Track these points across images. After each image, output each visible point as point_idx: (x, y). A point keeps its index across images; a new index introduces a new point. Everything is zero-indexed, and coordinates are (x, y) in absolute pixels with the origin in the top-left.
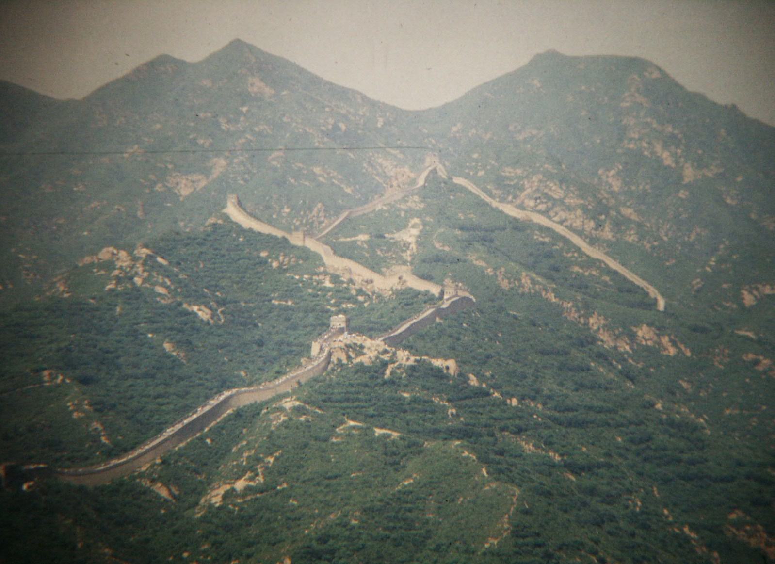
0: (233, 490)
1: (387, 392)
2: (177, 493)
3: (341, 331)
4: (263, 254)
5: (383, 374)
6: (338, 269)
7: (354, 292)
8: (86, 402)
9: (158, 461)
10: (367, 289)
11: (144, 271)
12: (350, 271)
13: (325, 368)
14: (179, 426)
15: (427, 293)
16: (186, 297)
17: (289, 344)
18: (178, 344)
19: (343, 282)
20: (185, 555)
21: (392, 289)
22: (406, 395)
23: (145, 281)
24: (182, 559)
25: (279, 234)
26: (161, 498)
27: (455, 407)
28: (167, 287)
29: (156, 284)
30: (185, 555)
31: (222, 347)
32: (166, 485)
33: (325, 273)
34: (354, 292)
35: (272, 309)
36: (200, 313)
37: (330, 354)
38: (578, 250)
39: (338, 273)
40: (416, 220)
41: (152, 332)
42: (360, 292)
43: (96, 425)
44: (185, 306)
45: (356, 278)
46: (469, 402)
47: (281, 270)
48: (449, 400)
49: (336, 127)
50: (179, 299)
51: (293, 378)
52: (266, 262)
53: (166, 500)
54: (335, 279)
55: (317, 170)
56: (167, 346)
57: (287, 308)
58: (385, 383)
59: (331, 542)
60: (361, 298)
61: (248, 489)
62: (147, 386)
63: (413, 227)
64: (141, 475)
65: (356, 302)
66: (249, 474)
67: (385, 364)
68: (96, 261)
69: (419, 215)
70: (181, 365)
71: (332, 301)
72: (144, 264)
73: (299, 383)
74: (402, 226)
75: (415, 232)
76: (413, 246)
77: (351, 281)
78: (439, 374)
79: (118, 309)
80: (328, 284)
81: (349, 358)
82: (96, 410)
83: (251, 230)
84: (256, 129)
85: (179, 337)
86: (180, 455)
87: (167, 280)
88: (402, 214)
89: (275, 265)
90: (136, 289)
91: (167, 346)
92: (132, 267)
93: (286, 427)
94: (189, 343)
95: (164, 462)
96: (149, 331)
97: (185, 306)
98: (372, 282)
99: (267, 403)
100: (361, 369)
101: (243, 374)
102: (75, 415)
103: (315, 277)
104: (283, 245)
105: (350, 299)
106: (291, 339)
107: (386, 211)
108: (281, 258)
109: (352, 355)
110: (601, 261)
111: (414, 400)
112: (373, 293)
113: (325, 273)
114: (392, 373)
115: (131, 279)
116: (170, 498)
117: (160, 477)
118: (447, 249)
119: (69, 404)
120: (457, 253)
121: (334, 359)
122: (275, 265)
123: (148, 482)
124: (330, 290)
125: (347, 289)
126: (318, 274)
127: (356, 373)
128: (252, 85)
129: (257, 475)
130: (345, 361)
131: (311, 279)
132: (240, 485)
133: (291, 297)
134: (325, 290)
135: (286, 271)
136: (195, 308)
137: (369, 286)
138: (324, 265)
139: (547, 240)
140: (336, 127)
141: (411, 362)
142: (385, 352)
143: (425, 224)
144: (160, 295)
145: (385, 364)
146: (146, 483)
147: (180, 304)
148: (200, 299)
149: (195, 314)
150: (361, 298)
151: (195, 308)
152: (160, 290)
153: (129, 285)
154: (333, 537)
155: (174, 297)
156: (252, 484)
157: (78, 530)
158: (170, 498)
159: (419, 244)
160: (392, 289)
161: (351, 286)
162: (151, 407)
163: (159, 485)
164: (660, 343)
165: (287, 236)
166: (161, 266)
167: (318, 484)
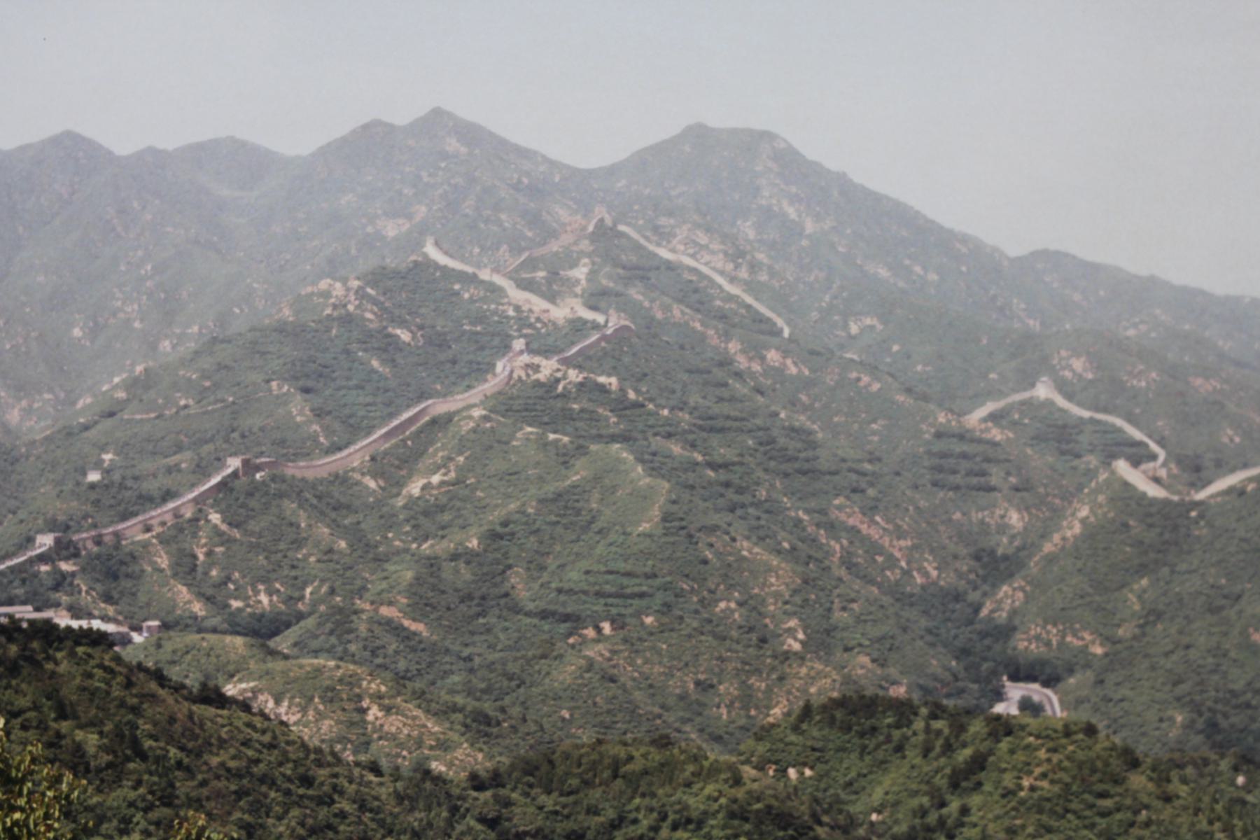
0: (430, 483)
1: (559, 404)
3: (522, 352)
4: (457, 287)
5: (556, 388)
7: (533, 320)
9: (367, 458)
10: (544, 317)
12: (528, 301)
13: (508, 383)
14: (383, 431)
15: (594, 321)
16: (393, 321)
17: (479, 363)
18: (383, 362)
20: (390, 535)
22: (575, 406)
23: (357, 307)
25: (469, 269)
28: (375, 314)
30: (390, 535)
32: (374, 477)
33: (510, 304)
34: (533, 320)
35: (464, 332)
36: (403, 336)
37: (512, 372)
38: (720, 287)
40: (586, 260)
42: (538, 320)
43: (316, 427)
44: (390, 329)
45: (535, 309)
46: (628, 412)
47: (472, 300)
48: (611, 411)
49: (519, 181)
50: (385, 324)
54: (518, 308)
55: (503, 217)
56: (375, 363)
57: (477, 333)
58: (558, 396)
59: (512, 526)
60: (539, 325)
61: (442, 483)
62: (358, 395)
63: (585, 265)
64: (353, 470)
66: (443, 471)
67: (558, 381)
69: (589, 255)
70: (387, 379)
73: (486, 396)
74: (573, 265)
75: (585, 270)
76: (583, 282)
77: (531, 311)
78: (603, 389)
79: (334, 331)
80: (511, 313)
81: (528, 375)
83: (445, 267)
85: (384, 356)
86: (386, 453)
88: (575, 255)
90: (349, 314)
91: (375, 363)
94: (393, 361)
95: (373, 459)
96: (359, 349)
97: (390, 329)
98: (548, 311)
99: (458, 412)
100: (538, 384)
101: (439, 387)
102: (298, 419)
104: (472, 279)
105: (531, 326)
106: (479, 359)
109: (530, 372)
110: (738, 297)
111: (582, 410)
113: (510, 304)
114: (564, 388)
115: (345, 306)
118: (611, 285)
120: (620, 288)
121: (515, 376)
122: (466, 296)
125: (528, 317)
126: (503, 304)
127: (534, 387)
130: (524, 378)
132: (436, 479)
133: (481, 323)
134: (507, 317)
135: (476, 301)
136: (398, 332)
138: (507, 297)
139: (694, 278)
140: (519, 181)
141: (580, 379)
142: (558, 370)
143: (593, 263)
145: (558, 381)
146: (357, 476)
147: (385, 328)
148: (403, 323)
150: (539, 325)
151: (398, 332)
152: (369, 315)
153: (343, 311)
154: (514, 522)
155: (381, 321)
156: (446, 478)
157: (301, 512)
159: (588, 280)
162: (361, 413)
164: (784, 364)
165: (477, 272)
167: (501, 479)
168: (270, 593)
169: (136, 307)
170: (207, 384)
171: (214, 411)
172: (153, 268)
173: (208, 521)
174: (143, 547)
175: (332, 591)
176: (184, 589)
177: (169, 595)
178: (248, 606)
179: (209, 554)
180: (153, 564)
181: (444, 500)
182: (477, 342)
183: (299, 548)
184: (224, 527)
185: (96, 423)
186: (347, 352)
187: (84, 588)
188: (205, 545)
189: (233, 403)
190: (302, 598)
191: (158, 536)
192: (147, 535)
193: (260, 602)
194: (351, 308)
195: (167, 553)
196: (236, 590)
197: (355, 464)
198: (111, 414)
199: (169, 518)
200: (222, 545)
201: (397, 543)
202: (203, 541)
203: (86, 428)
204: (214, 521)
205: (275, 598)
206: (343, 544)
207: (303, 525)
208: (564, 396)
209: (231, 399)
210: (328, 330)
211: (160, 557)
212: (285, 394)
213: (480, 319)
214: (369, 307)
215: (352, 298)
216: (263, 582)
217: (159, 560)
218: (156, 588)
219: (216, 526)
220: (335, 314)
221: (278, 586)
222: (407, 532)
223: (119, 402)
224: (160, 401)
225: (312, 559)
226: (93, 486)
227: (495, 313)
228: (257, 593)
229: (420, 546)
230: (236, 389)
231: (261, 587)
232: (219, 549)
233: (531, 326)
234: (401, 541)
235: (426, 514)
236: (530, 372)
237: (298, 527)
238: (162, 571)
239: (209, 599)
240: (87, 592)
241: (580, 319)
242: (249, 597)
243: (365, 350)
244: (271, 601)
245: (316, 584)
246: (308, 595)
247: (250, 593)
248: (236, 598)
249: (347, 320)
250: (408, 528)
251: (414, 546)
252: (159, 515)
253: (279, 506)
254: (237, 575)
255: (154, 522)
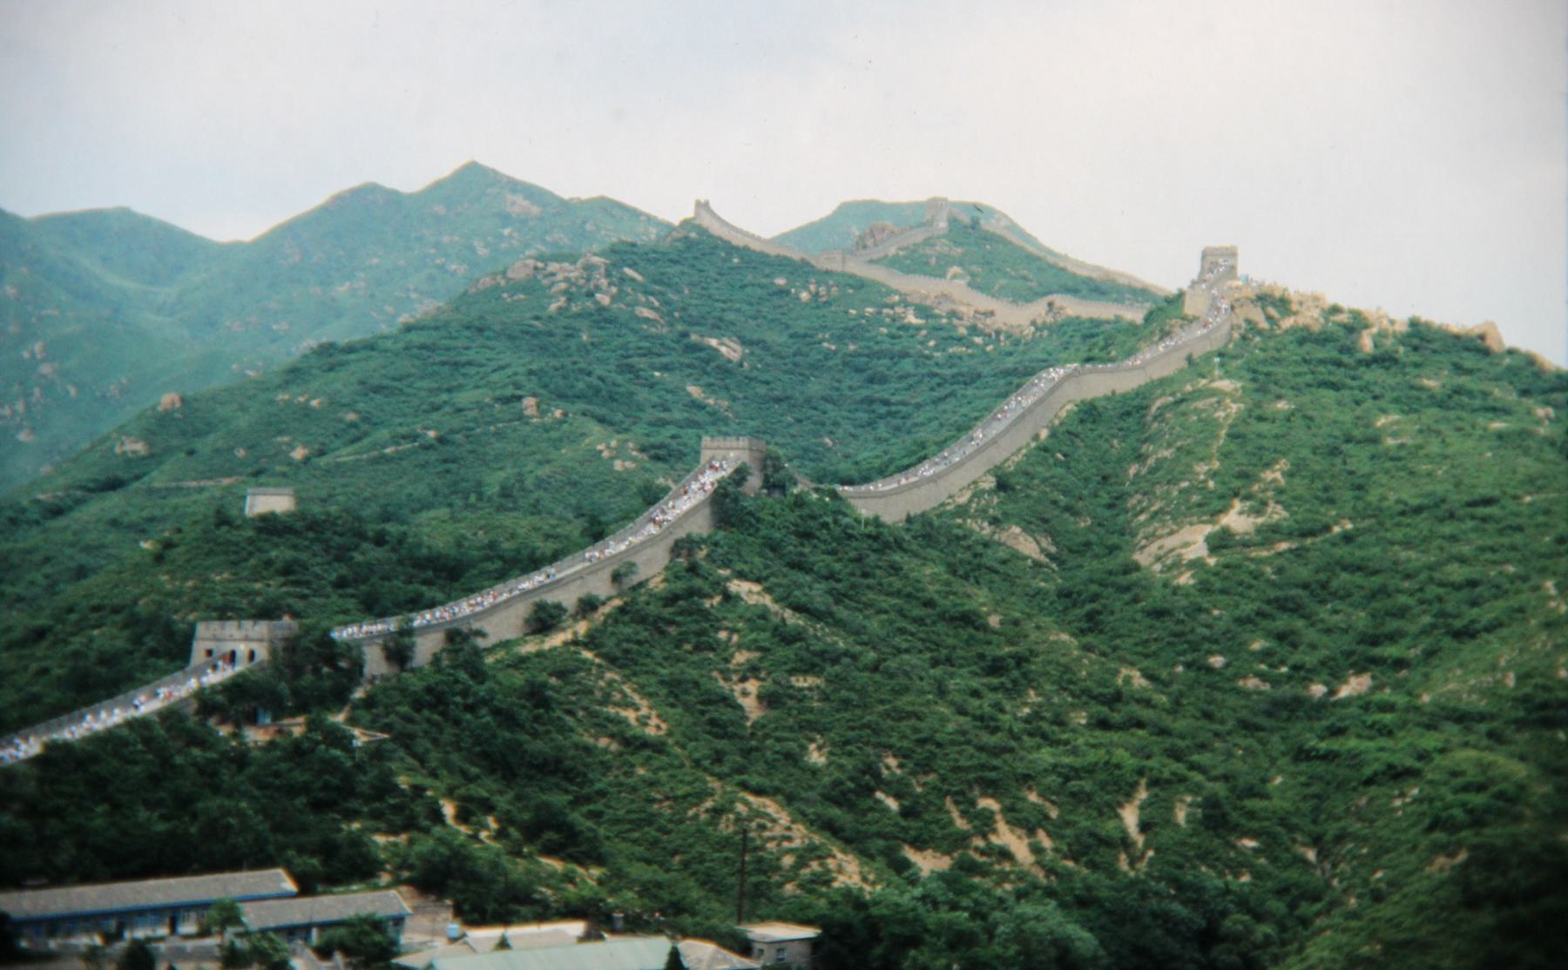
2: (1053, 549)
6: (926, 297)
7: (963, 331)
8: (631, 445)
10: (991, 324)
11: (610, 284)
17: (886, 403)
19: (940, 317)
21: (1033, 323)
23: (614, 299)
24: (1210, 670)
26: (1025, 558)
27: (1548, 403)
29: (637, 303)
30: (1217, 661)
31: (778, 400)
32: (1028, 528)
35: (828, 355)
36: (723, 349)
39: (928, 303)
40: (956, 269)
41: (659, 369)
42: (974, 330)
45: (963, 309)
50: (680, 327)
51: (1176, 349)
52: (788, 293)
53: (1037, 565)
54: (922, 311)
56: (694, 391)
58: (1369, 362)
60: (978, 340)
61: (1270, 534)
63: (955, 277)
64: (962, 511)
65: (971, 345)
68: (503, 283)
71: (932, 343)
72: (608, 275)
73: (1190, 359)
77: (953, 314)
80: (912, 319)
81: (1269, 318)
82: (657, 458)
83: (746, 248)
84: (548, 238)
85: (706, 379)
87: (652, 299)
89: (804, 296)
90: (601, 309)
91: (694, 391)
92: (588, 280)
93: (1261, 419)
95: (1003, 486)
97: (694, 338)
98: (992, 313)
102: (618, 465)
103: (885, 311)
106: (886, 396)
107: (906, 257)
108: (812, 288)
109: (1272, 311)
112: (998, 333)
114: (1376, 346)
115: (590, 295)
116: (1043, 559)
117: (1005, 514)
119: (600, 447)
123: (986, 524)
124: (918, 328)
127: (1302, 342)
128: (513, 203)
129: (1264, 504)
130: (1264, 325)
131: (880, 313)
133: (854, 339)
134: (905, 328)
137: (989, 321)
138: (890, 292)
143: (973, 275)
144: (647, 320)
147: (685, 335)
149: (716, 350)
150: (978, 340)
151: (714, 342)
152: (646, 313)
153: (589, 304)
155: (671, 325)
158: (1043, 559)
160: (1033, 323)
161: (955, 321)
163: (1017, 530)
166: (633, 280)
168: (1028, 824)
169: (20, 407)
170: (351, 417)
171: (400, 457)
172: (45, 349)
173: (728, 597)
174: (561, 674)
175: (1215, 819)
176: (770, 806)
177: (726, 827)
178: (970, 868)
179: (769, 699)
180: (604, 725)
181: (1303, 573)
182: (858, 370)
183: (1014, 691)
184: (792, 619)
185: (79, 502)
186: (631, 369)
187: (449, 809)
188: (752, 670)
189: (441, 440)
190: (1125, 843)
191: (591, 641)
192: (557, 640)
193: (1005, 854)
194: (604, 300)
195: (641, 690)
196: (906, 813)
197: (963, 500)
198: (113, 485)
199: (600, 587)
200: (810, 669)
201: (1252, 683)
202: (741, 657)
203: (57, 511)
204: (752, 600)
205: (1047, 843)
206: (1139, 681)
207: (994, 621)
208: (1383, 360)
209: (432, 434)
210: (571, 334)
211: (628, 704)
212: (561, 422)
213: (851, 332)
214: (642, 298)
215: (604, 282)
216: (991, 787)
217: (630, 715)
218: (666, 809)
219: (764, 615)
220: (574, 309)
221: (1033, 797)
222: (1265, 655)
223: (130, 461)
224: (241, 453)
225: (1081, 718)
226: (269, 525)
227: (877, 320)
228: (985, 823)
229: (1332, 692)
230: (435, 416)
231: (988, 803)
232: (801, 682)
233: (959, 340)
234: (1262, 676)
235: (1283, 605)
236: (1272, 311)
237: (985, 628)
238: (658, 747)
239: (853, 841)
240: (463, 816)
241: (1075, 322)
242: (961, 840)
243: (665, 368)
244: (1037, 850)
245: (1143, 795)
246: (1140, 840)
247: (961, 824)
248: (919, 844)
249: (602, 318)
250: (1257, 645)
251: (1318, 690)
252: (579, 576)
253: (895, 569)
254: (892, 762)
255: (568, 598)
